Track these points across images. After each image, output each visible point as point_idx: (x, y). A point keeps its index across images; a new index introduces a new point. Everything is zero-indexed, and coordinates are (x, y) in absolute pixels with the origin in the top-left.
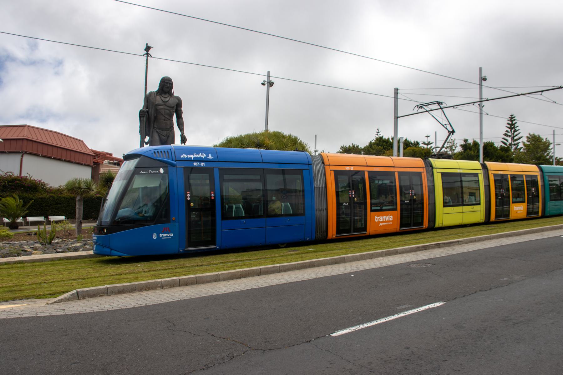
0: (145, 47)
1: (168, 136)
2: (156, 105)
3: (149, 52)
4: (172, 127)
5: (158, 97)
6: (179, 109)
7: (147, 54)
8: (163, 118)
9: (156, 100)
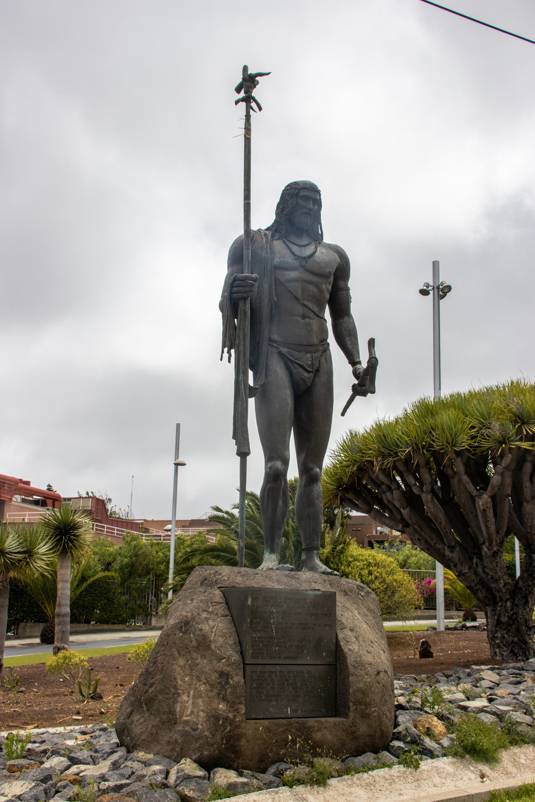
0: (239, 79)
1: (318, 370)
2: (276, 268)
3: (255, 93)
4: (324, 341)
5: (278, 245)
6: (341, 283)
7: (248, 99)
8: (300, 310)
9: (273, 252)
